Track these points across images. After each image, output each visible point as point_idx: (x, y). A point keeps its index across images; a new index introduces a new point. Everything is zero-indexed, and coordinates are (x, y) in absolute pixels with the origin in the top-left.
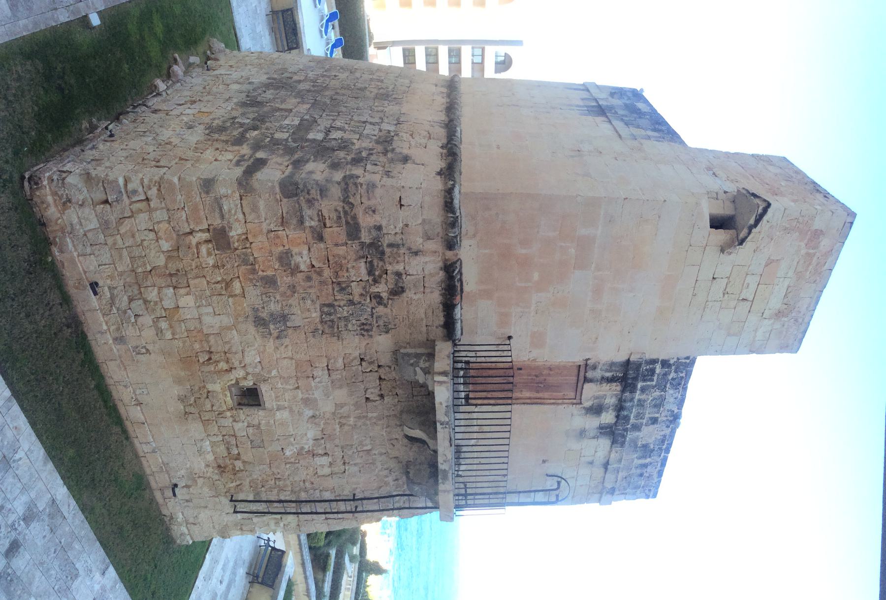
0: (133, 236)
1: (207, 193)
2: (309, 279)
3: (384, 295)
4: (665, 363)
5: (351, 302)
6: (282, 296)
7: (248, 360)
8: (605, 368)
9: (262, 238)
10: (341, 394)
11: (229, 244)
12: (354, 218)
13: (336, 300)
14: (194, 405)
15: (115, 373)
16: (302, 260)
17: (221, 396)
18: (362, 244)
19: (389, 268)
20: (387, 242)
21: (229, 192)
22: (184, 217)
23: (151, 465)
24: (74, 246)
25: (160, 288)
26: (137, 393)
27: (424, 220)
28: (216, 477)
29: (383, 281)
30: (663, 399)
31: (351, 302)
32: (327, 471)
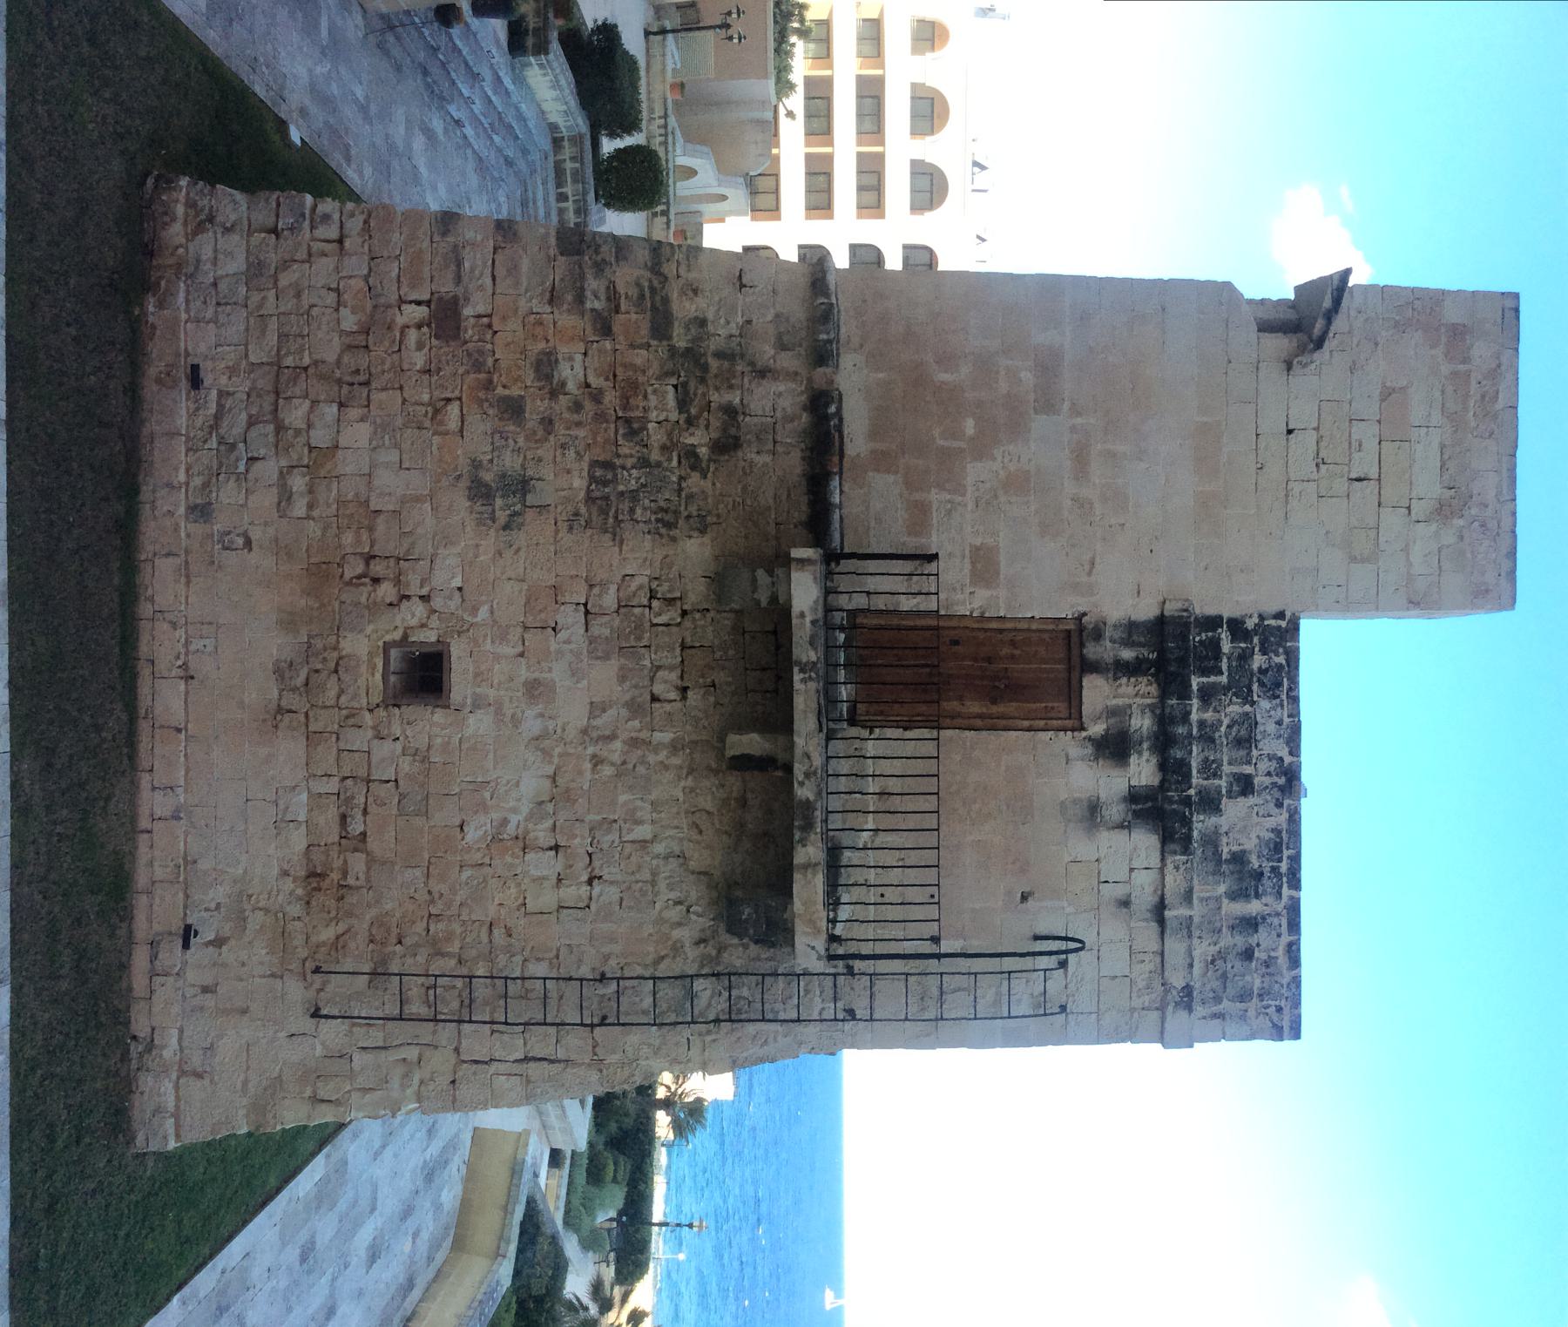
0: (298, 295)
1: (444, 234)
2: (577, 407)
3: (703, 451)
4: (1237, 628)
5: (644, 463)
6: (527, 438)
7: (439, 578)
8: (1117, 635)
9: (514, 325)
10: (604, 677)
11: (458, 328)
12: (666, 301)
13: (619, 456)
14: (305, 682)
15: (163, 585)
16: (571, 373)
17: (363, 669)
18: (673, 351)
19: (715, 397)
20: (712, 347)
21: (479, 238)
22: (394, 274)
23: (153, 861)
24: (187, 301)
25: (315, 402)
26: (192, 648)
27: (777, 316)
28: (295, 910)
29: (702, 422)
30: (1250, 722)
31: (644, 463)
32: (547, 899)
